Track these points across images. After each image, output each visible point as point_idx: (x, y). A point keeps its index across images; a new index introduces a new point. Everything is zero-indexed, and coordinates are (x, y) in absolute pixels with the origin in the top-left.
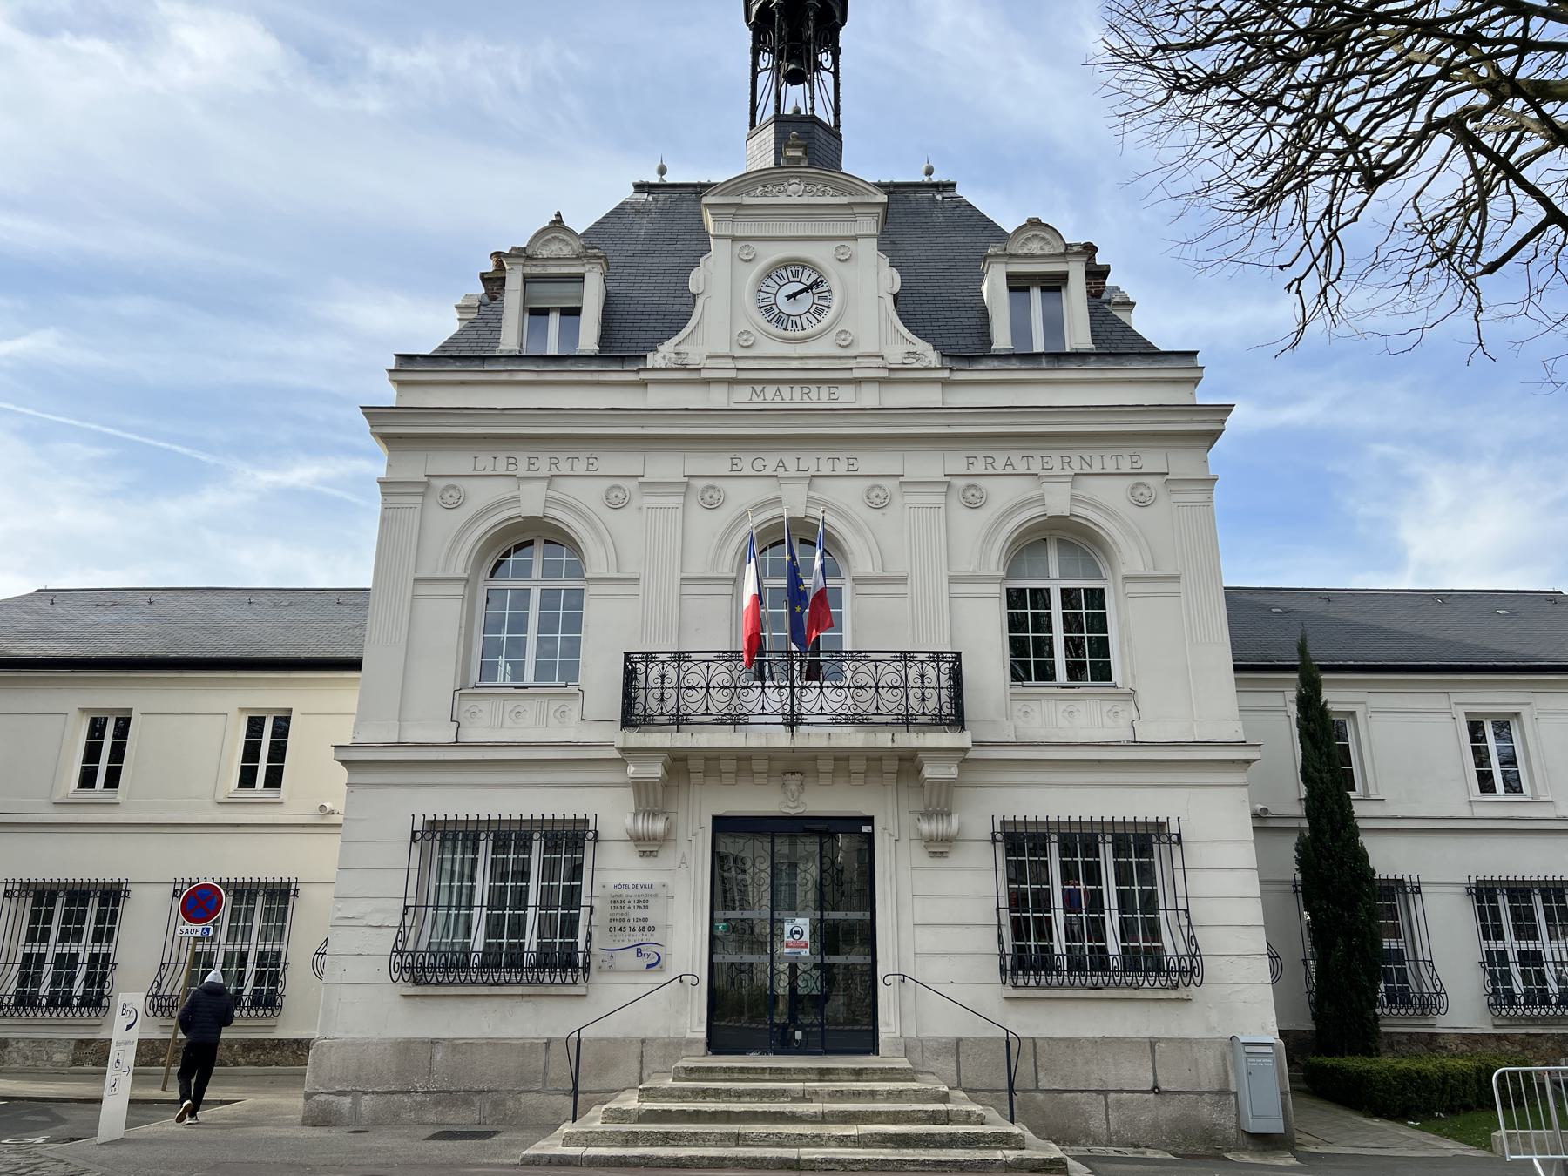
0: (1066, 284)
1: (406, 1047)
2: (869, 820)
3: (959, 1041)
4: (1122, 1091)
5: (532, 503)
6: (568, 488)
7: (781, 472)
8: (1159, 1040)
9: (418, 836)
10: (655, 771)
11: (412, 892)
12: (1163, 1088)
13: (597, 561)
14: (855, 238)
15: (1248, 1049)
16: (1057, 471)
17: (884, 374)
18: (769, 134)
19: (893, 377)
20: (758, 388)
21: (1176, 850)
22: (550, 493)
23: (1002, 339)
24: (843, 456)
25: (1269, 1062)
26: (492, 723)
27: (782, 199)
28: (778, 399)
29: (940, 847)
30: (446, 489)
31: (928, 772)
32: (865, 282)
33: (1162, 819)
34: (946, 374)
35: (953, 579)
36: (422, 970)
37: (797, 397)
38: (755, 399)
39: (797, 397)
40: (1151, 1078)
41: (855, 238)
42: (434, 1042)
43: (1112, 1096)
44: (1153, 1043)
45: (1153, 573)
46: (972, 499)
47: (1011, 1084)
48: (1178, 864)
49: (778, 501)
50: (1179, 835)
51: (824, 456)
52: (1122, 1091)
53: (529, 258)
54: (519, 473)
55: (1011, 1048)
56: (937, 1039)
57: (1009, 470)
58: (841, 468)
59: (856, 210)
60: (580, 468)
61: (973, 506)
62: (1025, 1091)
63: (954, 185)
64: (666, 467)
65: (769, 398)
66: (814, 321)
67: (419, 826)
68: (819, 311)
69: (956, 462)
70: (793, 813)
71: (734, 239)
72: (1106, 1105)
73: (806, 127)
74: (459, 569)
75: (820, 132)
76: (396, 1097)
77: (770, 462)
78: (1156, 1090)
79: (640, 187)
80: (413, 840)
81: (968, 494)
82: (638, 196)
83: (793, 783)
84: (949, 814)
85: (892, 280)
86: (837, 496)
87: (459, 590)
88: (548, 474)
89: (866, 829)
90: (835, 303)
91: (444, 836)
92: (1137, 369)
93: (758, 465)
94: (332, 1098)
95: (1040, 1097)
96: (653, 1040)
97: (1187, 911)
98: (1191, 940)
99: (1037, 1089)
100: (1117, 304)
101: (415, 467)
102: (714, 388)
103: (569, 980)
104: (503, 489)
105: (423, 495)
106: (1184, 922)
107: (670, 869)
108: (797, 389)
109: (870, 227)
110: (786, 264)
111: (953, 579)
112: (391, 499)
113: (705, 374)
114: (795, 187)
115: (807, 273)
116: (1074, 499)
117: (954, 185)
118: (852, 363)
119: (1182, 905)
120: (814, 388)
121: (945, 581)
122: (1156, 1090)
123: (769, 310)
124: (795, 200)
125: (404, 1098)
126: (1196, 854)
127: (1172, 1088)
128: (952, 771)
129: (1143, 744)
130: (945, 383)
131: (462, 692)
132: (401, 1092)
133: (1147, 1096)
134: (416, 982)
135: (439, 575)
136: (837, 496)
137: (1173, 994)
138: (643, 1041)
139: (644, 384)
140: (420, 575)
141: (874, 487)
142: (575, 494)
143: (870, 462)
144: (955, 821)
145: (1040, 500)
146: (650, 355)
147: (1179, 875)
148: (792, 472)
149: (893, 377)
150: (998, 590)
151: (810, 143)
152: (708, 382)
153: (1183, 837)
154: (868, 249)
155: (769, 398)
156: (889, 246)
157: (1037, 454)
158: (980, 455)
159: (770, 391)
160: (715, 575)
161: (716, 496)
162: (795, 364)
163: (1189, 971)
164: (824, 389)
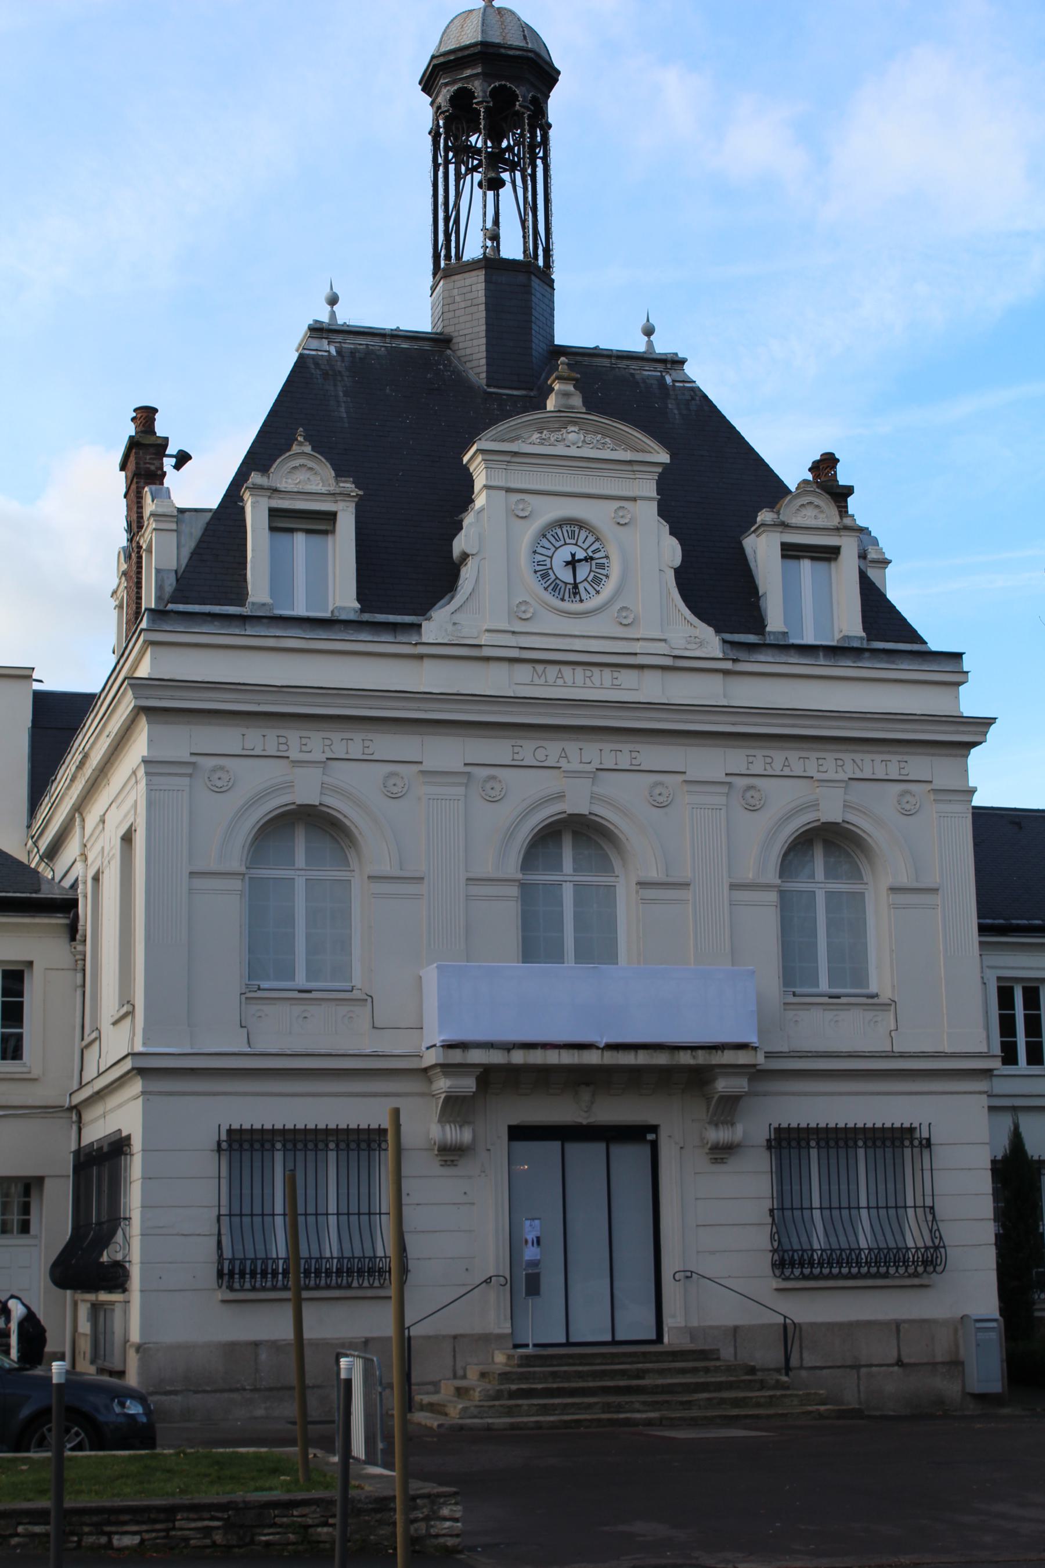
0: (836, 559)
1: (231, 1349)
2: (654, 1129)
3: (736, 1329)
4: (871, 1366)
5: (306, 794)
6: (345, 775)
7: (563, 763)
8: (905, 1321)
9: (224, 1145)
10: (468, 1084)
11: (224, 1201)
12: (906, 1360)
13: (376, 852)
14: (634, 499)
15: (979, 1325)
16: (831, 775)
17: (669, 662)
18: (476, 283)
19: (677, 666)
20: (540, 668)
21: (926, 1152)
22: (326, 779)
23: (775, 622)
24: (626, 747)
25: (993, 1335)
26: (288, 1031)
27: (560, 450)
28: (560, 682)
29: (722, 1152)
30: (214, 770)
31: (723, 1085)
32: (646, 552)
33: (916, 1125)
34: (728, 665)
35: (733, 887)
36: (241, 1275)
37: (579, 681)
38: (537, 681)
39: (579, 681)
40: (895, 1354)
41: (634, 499)
42: (256, 1344)
43: (864, 1370)
44: (898, 1325)
45: (915, 885)
46: (752, 802)
47: (787, 1359)
48: (927, 1165)
49: (560, 797)
50: (928, 1140)
51: (607, 747)
52: (871, 1366)
53: (276, 490)
54: (294, 754)
55: (789, 1334)
56: (717, 1328)
57: (787, 772)
58: (624, 763)
59: (636, 468)
60: (356, 752)
61: (754, 810)
62: (795, 1368)
63: (683, 362)
64: (445, 753)
65: (551, 681)
66: (593, 592)
67: (224, 1137)
68: (597, 580)
69: (736, 759)
70: (585, 1122)
71: (509, 490)
72: (859, 1378)
73: (521, 278)
74: (236, 864)
75: (536, 283)
76: (226, 1395)
77: (552, 750)
78: (899, 1363)
79: (317, 330)
80: (219, 1149)
81: (749, 794)
82: (315, 344)
83: (585, 1094)
84: (733, 1124)
85: (672, 551)
86: (614, 787)
87: (236, 884)
88: (322, 757)
89: (650, 1137)
90: (615, 570)
91: (242, 1145)
92: (907, 670)
93: (540, 754)
94: (164, 1398)
95: (804, 1373)
96: (462, 1336)
97: (932, 1208)
98: (934, 1232)
99: (801, 1367)
100: (873, 561)
101: (184, 741)
102: (494, 666)
103: (377, 1284)
104: (271, 772)
105: (190, 775)
106: (930, 1218)
107: (470, 1177)
108: (579, 670)
109: (648, 488)
110: (561, 523)
111: (733, 887)
112: (156, 779)
113: (487, 652)
114: (573, 435)
115: (583, 534)
116: (846, 806)
117: (683, 362)
118: (637, 647)
119: (929, 1203)
120: (596, 671)
121: (726, 887)
122: (899, 1363)
123: (545, 576)
124: (573, 451)
125: (235, 1396)
126: (942, 1155)
127: (913, 1360)
128: (738, 1085)
129: (902, 1056)
130: (726, 672)
131: (252, 994)
132: (231, 1390)
133: (892, 1369)
134: (231, 1288)
135: (214, 867)
136: (614, 787)
137: (916, 1281)
138: (455, 1337)
139: (421, 657)
140: (195, 869)
141: (657, 784)
142: (346, 776)
143: (655, 755)
144: (739, 1129)
145: (814, 805)
146: (425, 624)
147: (927, 1174)
148: (575, 766)
149: (677, 666)
150: (773, 897)
151: (518, 288)
152: (488, 659)
153: (933, 1141)
154: (648, 512)
155: (551, 681)
156: (668, 510)
157: (813, 755)
158: (759, 753)
159: (552, 671)
160: (501, 875)
161: (497, 786)
162: (578, 644)
163: (931, 1261)
164: (607, 672)
